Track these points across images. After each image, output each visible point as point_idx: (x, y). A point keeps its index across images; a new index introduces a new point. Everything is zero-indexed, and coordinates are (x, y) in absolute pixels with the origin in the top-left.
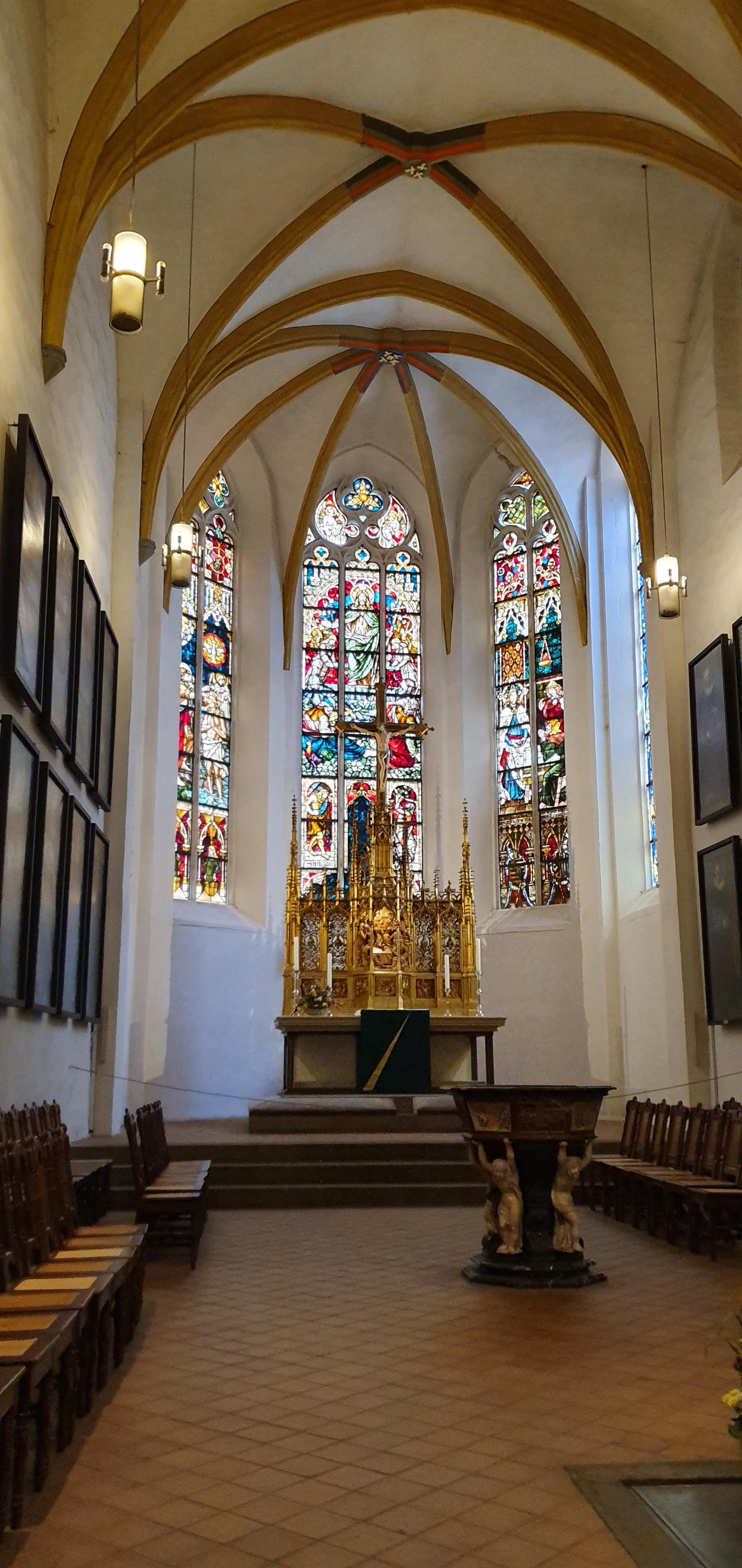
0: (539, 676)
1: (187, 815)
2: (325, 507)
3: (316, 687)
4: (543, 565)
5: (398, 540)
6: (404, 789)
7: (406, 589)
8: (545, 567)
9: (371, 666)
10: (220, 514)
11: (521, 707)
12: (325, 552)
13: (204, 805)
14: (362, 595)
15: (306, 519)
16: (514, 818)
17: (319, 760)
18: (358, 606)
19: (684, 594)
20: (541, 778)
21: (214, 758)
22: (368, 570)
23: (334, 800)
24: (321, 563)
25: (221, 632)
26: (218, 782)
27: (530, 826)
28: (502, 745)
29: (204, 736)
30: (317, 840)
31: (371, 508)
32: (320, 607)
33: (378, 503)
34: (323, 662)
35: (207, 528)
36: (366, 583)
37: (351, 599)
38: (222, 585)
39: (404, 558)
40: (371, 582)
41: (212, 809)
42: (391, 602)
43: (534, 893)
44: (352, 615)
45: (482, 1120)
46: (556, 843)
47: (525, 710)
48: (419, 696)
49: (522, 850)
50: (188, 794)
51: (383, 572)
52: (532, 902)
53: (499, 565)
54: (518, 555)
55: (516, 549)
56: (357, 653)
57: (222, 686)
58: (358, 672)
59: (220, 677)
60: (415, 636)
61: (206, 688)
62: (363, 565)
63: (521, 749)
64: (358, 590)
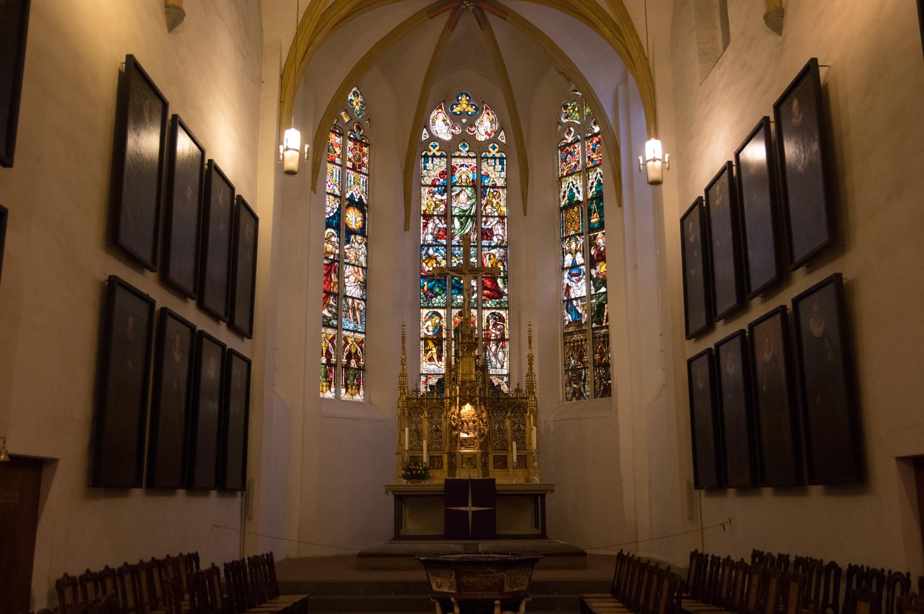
2: (436, 114)
3: (430, 242)
4: (592, 149)
5: (489, 135)
6: (495, 315)
7: (496, 170)
9: (470, 226)
10: (359, 123)
11: (578, 253)
12: (437, 146)
13: (347, 330)
14: (464, 175)
15: (422, 122)
16: (575, 334)
17: (433, 295)
18: (461, 183)
19: (667, 168)
20: (593, 305)
21: (355, 296)
22: (468, 157)
23: (444, 324)
24: (434, 154)
25: (360, 206)
27: (586, 340)
28: (566, 281)
29: (346, 280)
30: (432, 353)
31: (470, 113)
32: (434, 185)
33: (474, 109)
35: (349, 133)
36: (467, 166)
38: (360, 172)
39: (494, 148)
40: (471, 165)
41: (352, 333)
42: (485, 179)
43: (589, 389)
45: (437, 583)
46: (604, 353)
47: (581, 255)
49: (580, 358)
50: (335, 322)
51: (479, 158)
52: (587, 396)
53: (562, 151)
54: (575, 143)
55: (573, 139)
56: (460, 217)
57: (361, 244)
58: (461, 230)
59: (359, 238)
60: (502, 203)
61: (347, 246)
62: (464, 154)
63: (579, 284)
64: (461, 171)
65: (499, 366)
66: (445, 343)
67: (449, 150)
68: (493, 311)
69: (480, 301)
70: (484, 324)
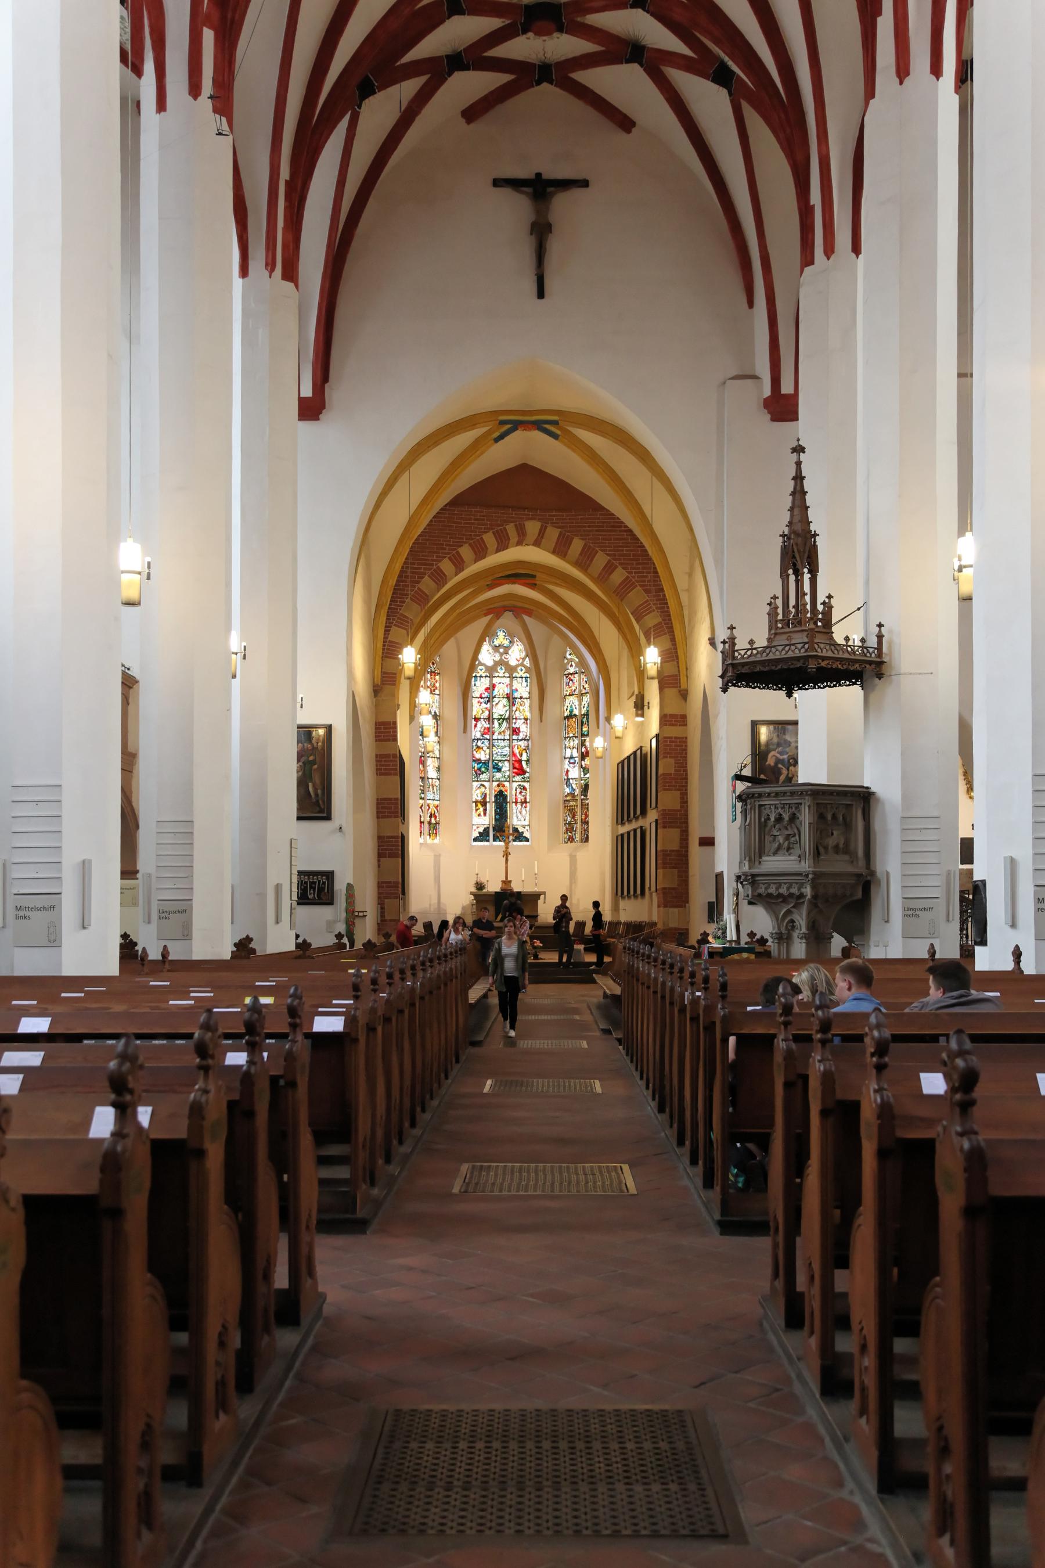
0: (583, 735)
1: (422, 805)
5: (519, 661)
8: (586, 682)
22: (504, 677)
23: (488, 792)
26: (435, 788)
32: (481, 697)
34: (483, 724)
37: (495, 693)
39: (522, 670)
44: (496, 700)
48: (528, 740)
49: (573, 817)
53: (567, 677)
56: (499, 719)
60: (527, 709)
65: (523, 819)
66: (488, 805)
67: (491, 671)
68: (520, 783)
69: (511, 777)
70: (514, 792)
